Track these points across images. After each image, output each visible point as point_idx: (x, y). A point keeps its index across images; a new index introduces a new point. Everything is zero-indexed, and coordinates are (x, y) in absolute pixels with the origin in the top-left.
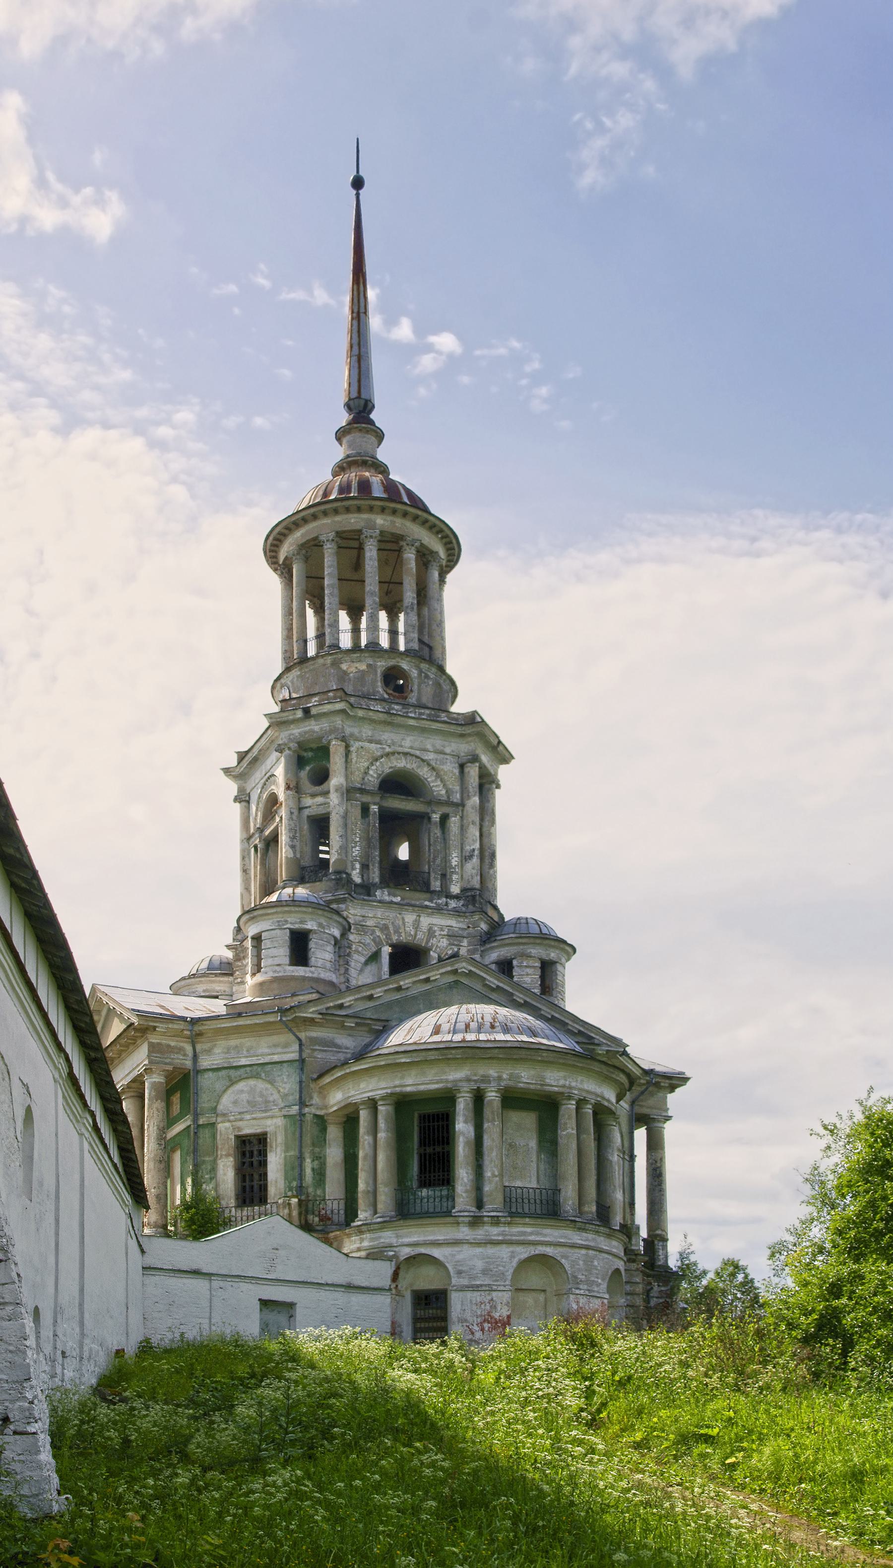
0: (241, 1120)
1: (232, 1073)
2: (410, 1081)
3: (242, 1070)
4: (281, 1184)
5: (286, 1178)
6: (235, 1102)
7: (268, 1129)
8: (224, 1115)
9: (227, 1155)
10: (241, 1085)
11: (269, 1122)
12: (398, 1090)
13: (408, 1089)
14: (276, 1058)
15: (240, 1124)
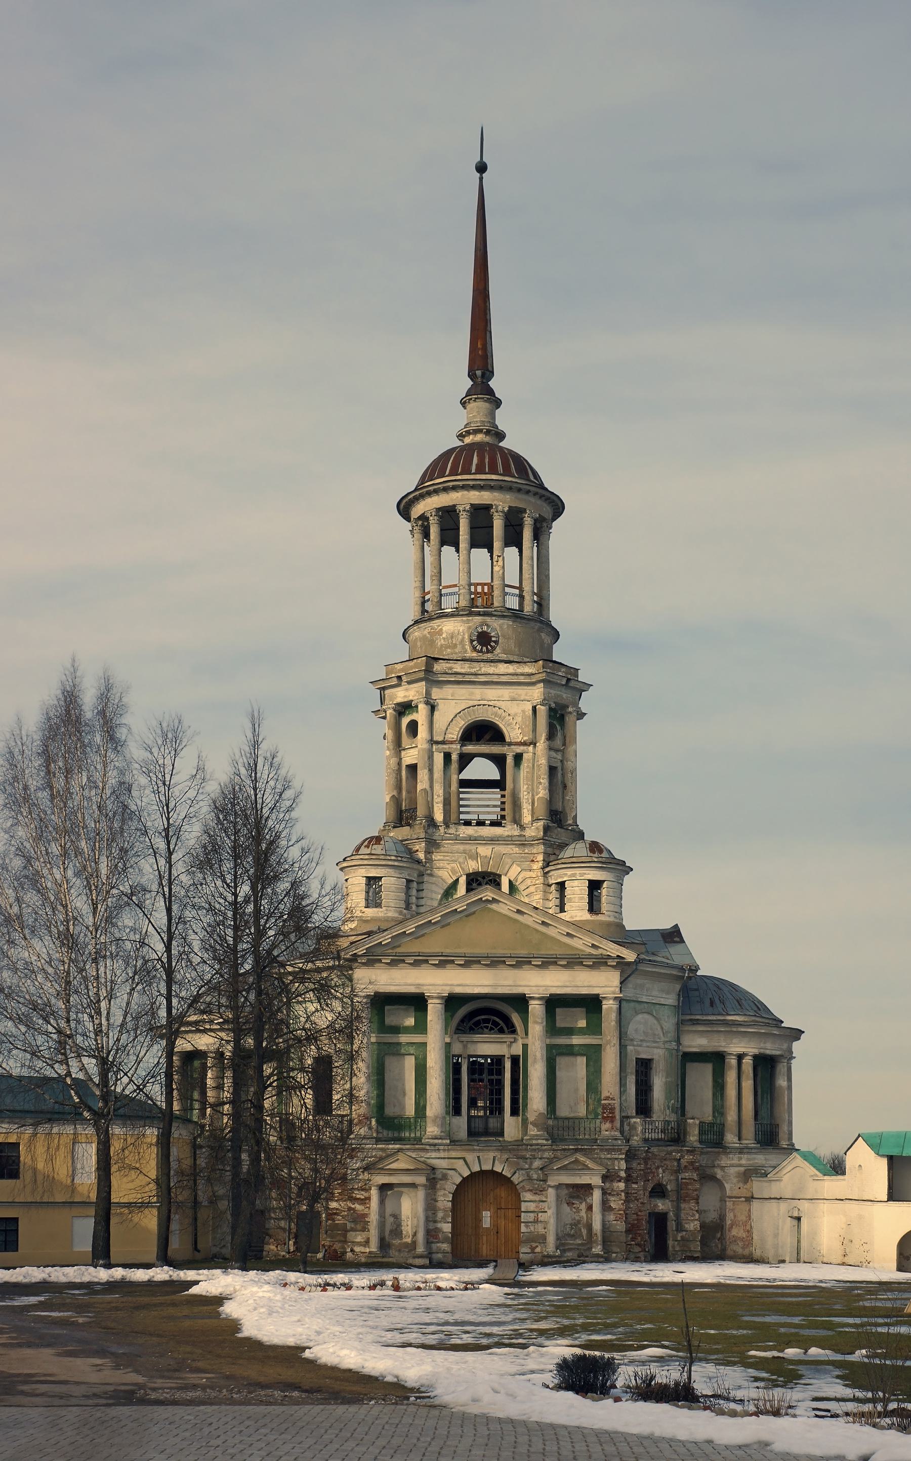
0: (640, 1046)
1: (637, 1005)
2: (769, 1045)
3: (643, 1005)
4: (662, 1101)
5: (666, 1098)
6: (636, 1030)
7: (655, 1057)
8: (632, 1040)
9: (631, 1073)
10: (640, 1017)
11: (656, 1051)
12: (762, 1051)
13: (768, 1052)
14: (663, 1001)
15: (639, 1048)
